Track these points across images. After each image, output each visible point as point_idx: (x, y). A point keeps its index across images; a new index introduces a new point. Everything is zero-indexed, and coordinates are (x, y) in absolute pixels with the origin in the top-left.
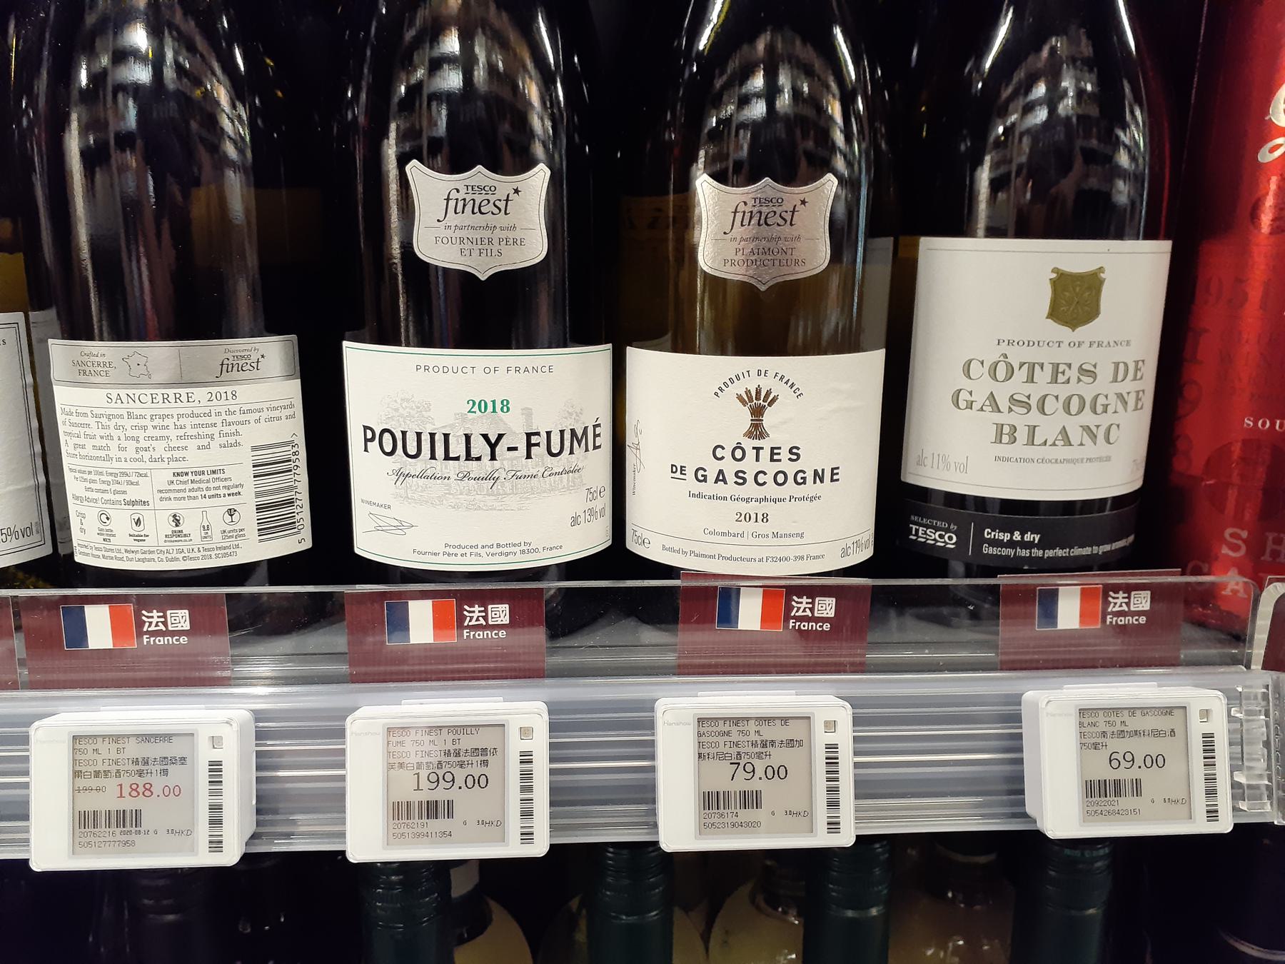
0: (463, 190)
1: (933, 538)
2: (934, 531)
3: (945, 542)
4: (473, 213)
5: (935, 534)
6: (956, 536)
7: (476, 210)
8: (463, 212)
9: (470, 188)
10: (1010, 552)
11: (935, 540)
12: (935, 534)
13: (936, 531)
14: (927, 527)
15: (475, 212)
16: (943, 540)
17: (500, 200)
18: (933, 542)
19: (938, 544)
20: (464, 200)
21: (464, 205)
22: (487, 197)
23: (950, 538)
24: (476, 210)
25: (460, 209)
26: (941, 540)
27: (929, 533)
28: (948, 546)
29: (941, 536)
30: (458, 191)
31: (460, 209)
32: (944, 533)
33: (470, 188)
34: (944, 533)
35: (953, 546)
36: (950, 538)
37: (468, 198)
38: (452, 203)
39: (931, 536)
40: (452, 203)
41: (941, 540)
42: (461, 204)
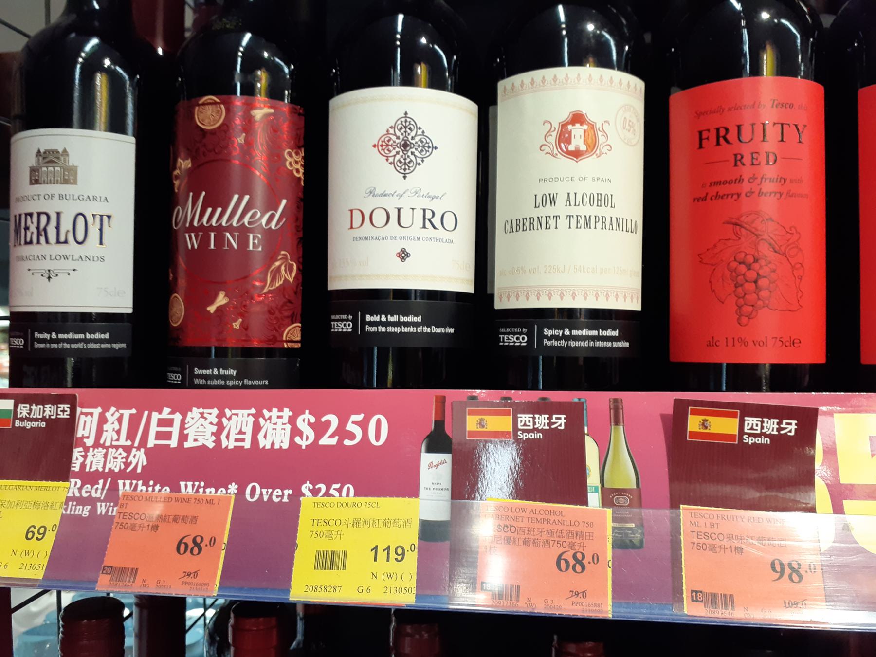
1: (513, 341)
2: (513, 336)
3: (521, 342)
5: (513, 337)
6: (527, 336)
11: (514, 342)
13: (514, 335)
14: (509, 334)
16: (519, 341)
18: (512, 344)
19: (516, 344)
26: (517, 341)
27: (510, 338)
28: (523, 344)
29: (518, 338)
32: (519, 336)
34: (519, 336)
35: (525, 344)
36: (523, 339)
39: (511, 340)
41: (517, 341)
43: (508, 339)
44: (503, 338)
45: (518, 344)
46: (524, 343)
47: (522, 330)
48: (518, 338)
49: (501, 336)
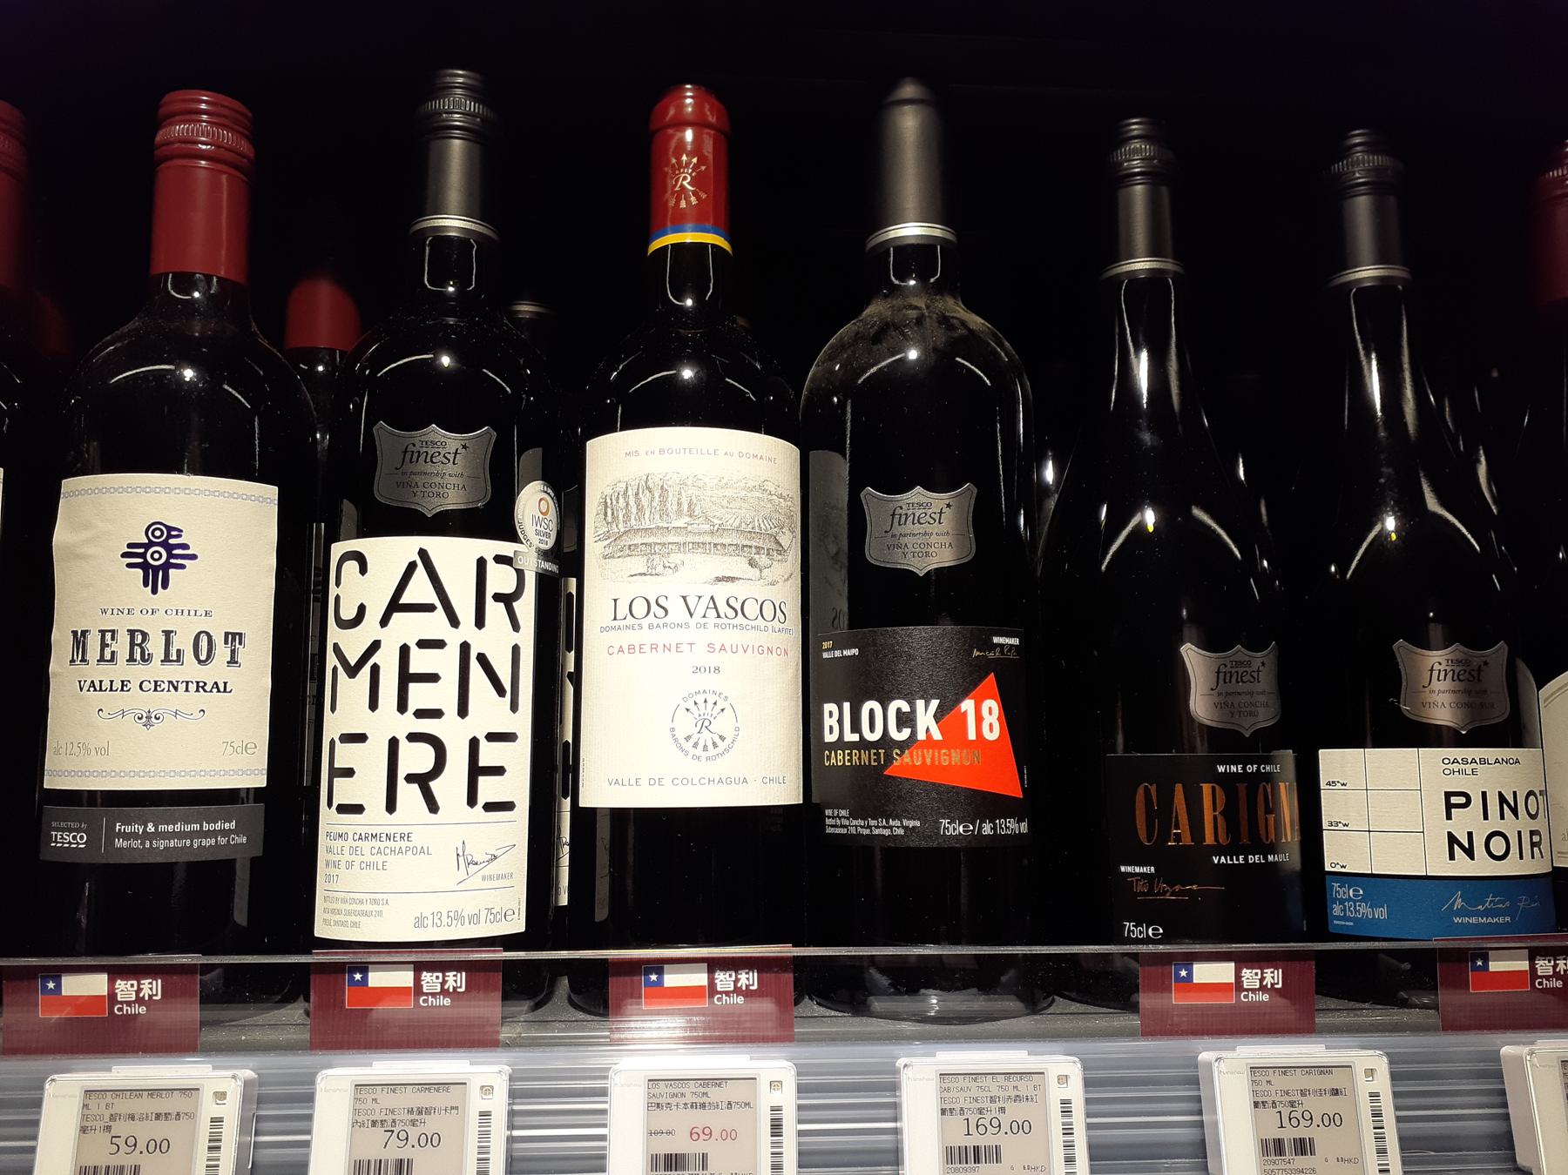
3: (78, 843)
5: (69, 836)
10: (136, 844)
11: (70, 843)
12: (69, 836)
14: (63, 830)
18: (67, 845)
23: (82, 838)
28: (81, 846)
29: (74, 838)
35: (83, 846)
36: (82, 838)
43: (63, 838)
44: (56, 835)
45: (74, 846)
46: (83, 844)
47: (81, 825)
48: (74, 838)
49: (54, 833)
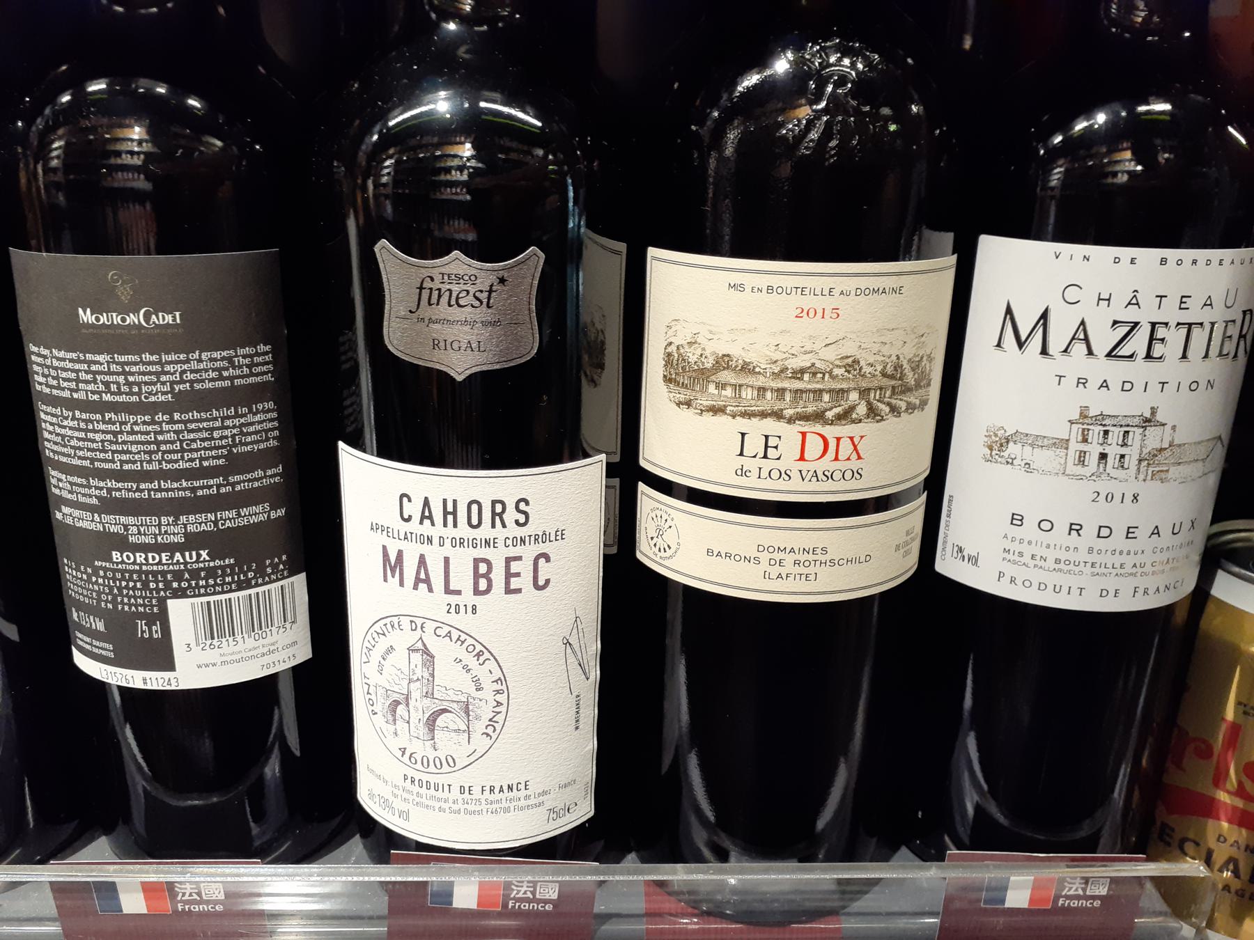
0: (438, 278)
4: (450, 305)
7: (453, 302)
8: (438, 304)
9: (446, 277)
15: (452, 303)
17: (481, 291)
20: (439, 290)
21: (440, 296)
22: (465, 287)
24: (453, 302)
25: (434, 300)
30: (432, 279)
31: (434, 300)
33: (446, 277)
37: (445, 287)
38: (425, 294)
40: (425, 294)
42: (435, 294)
